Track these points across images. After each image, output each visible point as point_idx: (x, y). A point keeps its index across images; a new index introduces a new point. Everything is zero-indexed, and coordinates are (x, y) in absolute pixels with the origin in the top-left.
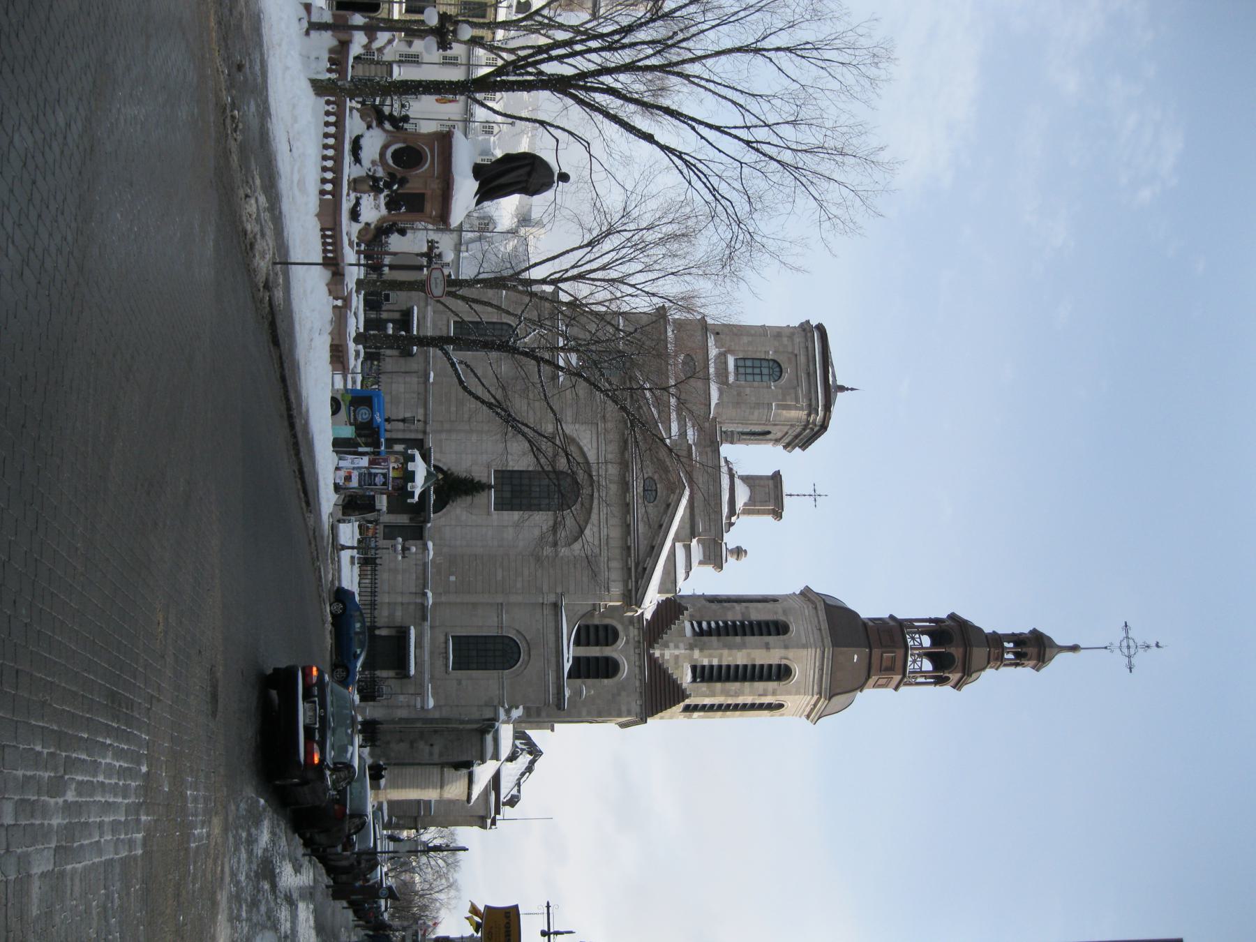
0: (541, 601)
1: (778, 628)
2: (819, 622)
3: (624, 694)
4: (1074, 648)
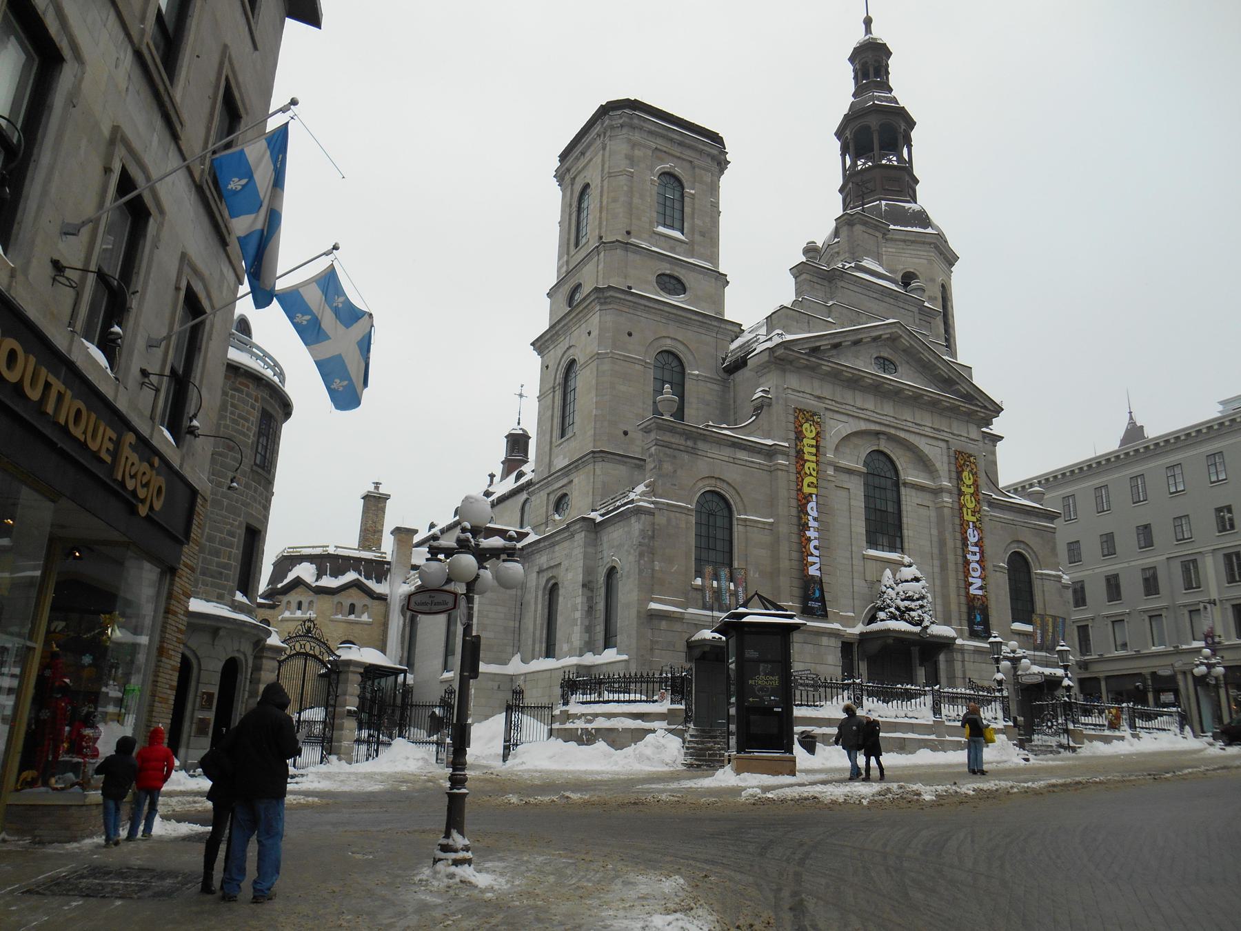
2: (904, 241)
4: (868, 22)
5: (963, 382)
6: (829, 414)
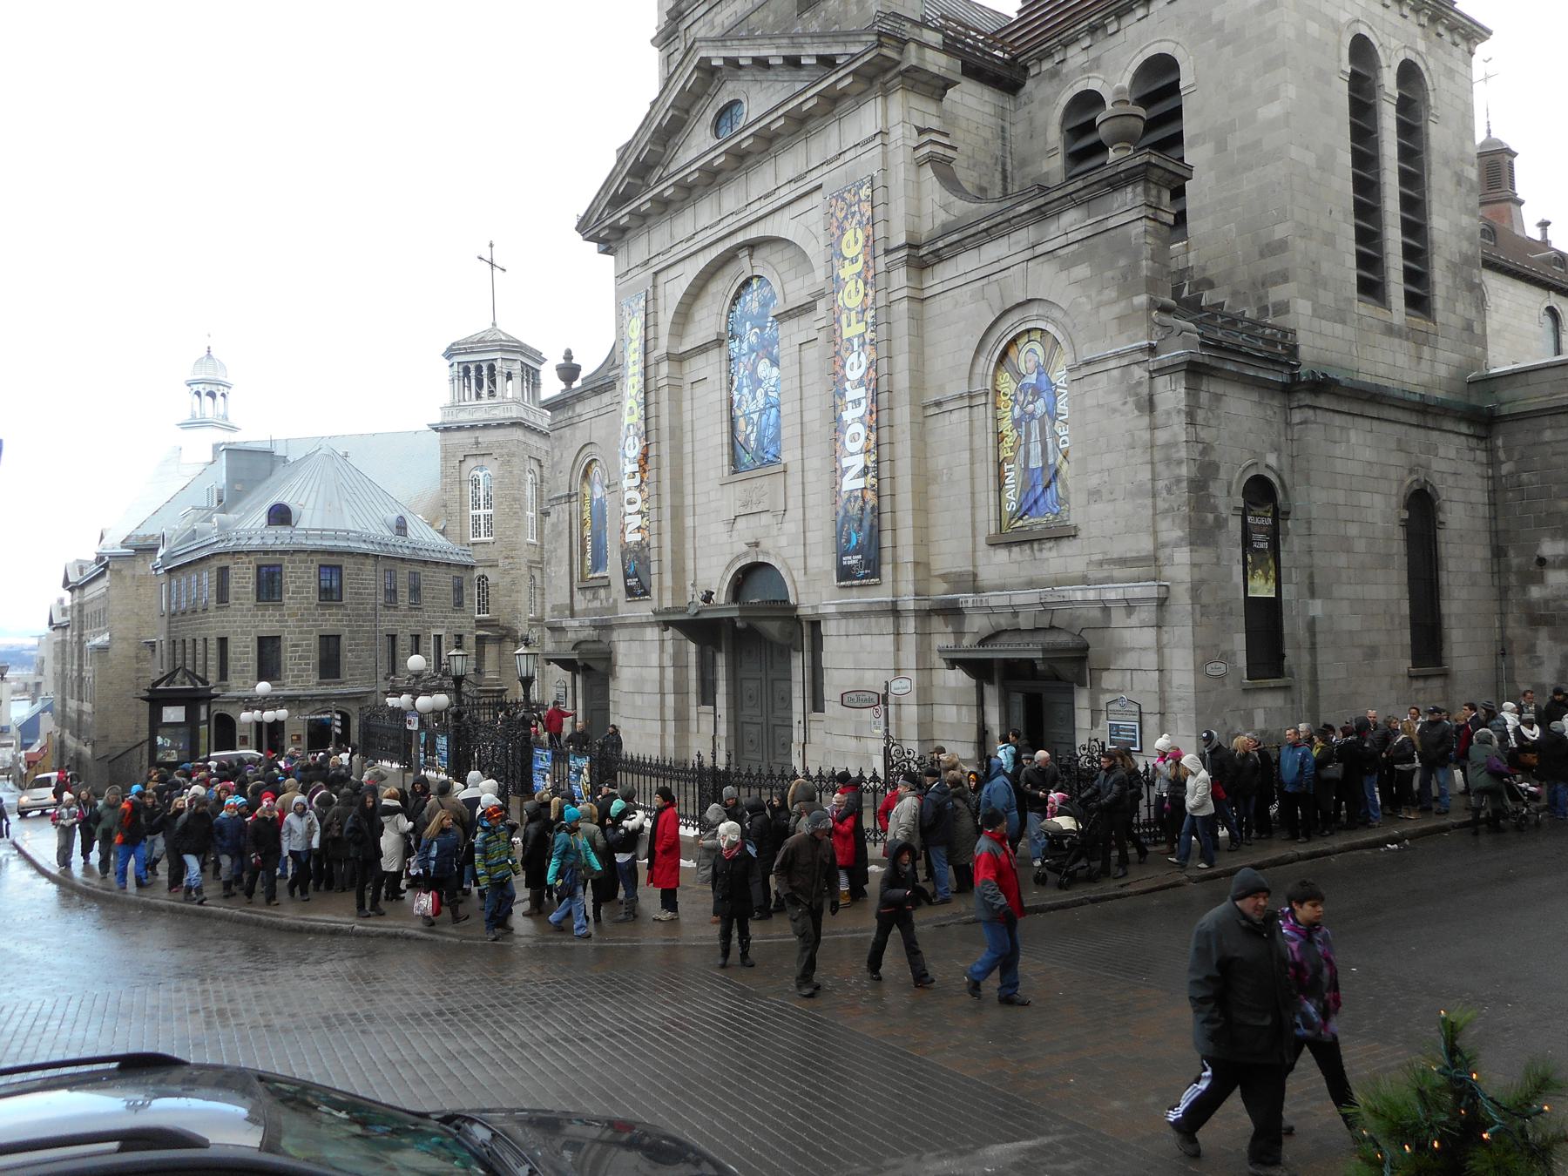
0: (905, 304)
3: (1216, 18)
5: (801, 46)
6: (662, 278)
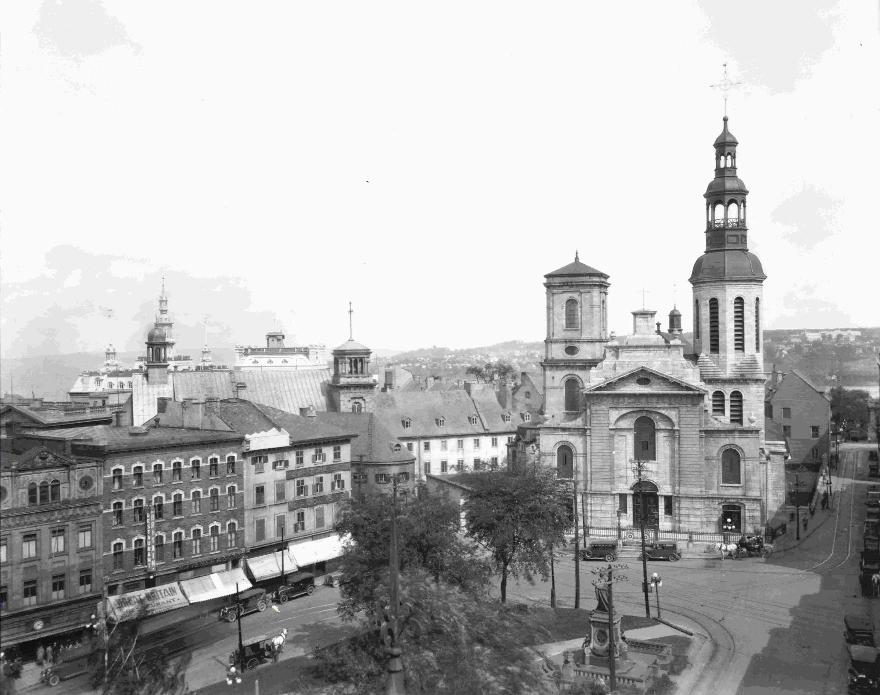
1: (714, 304)
4: (725, 120)
